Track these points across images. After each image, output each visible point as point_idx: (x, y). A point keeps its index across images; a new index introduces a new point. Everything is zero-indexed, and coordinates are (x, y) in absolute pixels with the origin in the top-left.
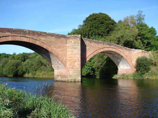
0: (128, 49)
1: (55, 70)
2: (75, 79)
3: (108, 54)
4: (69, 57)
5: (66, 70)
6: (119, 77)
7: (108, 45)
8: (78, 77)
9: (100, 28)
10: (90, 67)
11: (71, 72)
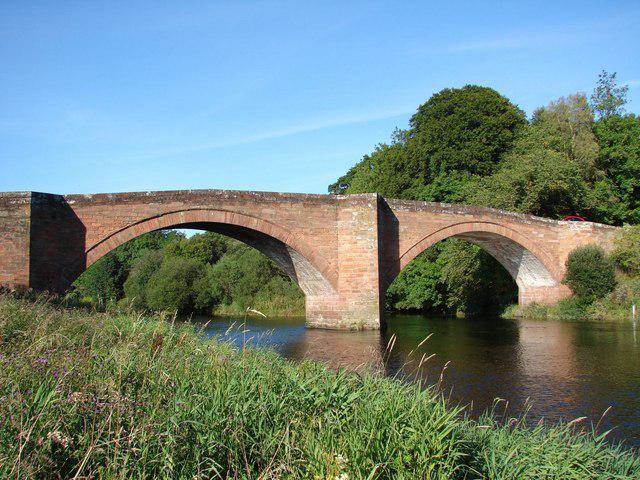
0: (544, 223)
1: (308, 297)
2: (362, 324)
9: (467, 143)
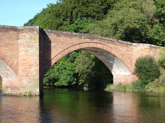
0: (126, 44)
1: (3, 79)
2: (30, 93)
3: (93, 52)
4: (22, 59)
5: (18, 78)
6: (114, 89)
7: (88, 38)
8: (35, 89)
9: (91, 4)
10: (71, 72)
11: (24, 82)
